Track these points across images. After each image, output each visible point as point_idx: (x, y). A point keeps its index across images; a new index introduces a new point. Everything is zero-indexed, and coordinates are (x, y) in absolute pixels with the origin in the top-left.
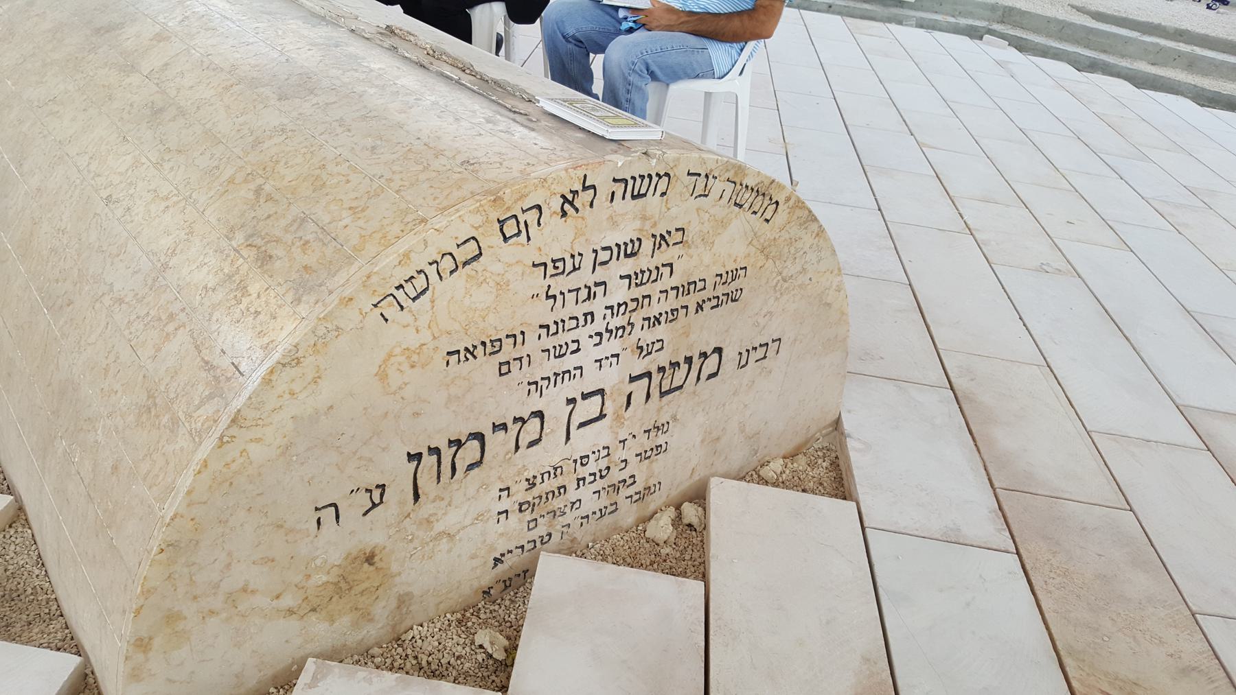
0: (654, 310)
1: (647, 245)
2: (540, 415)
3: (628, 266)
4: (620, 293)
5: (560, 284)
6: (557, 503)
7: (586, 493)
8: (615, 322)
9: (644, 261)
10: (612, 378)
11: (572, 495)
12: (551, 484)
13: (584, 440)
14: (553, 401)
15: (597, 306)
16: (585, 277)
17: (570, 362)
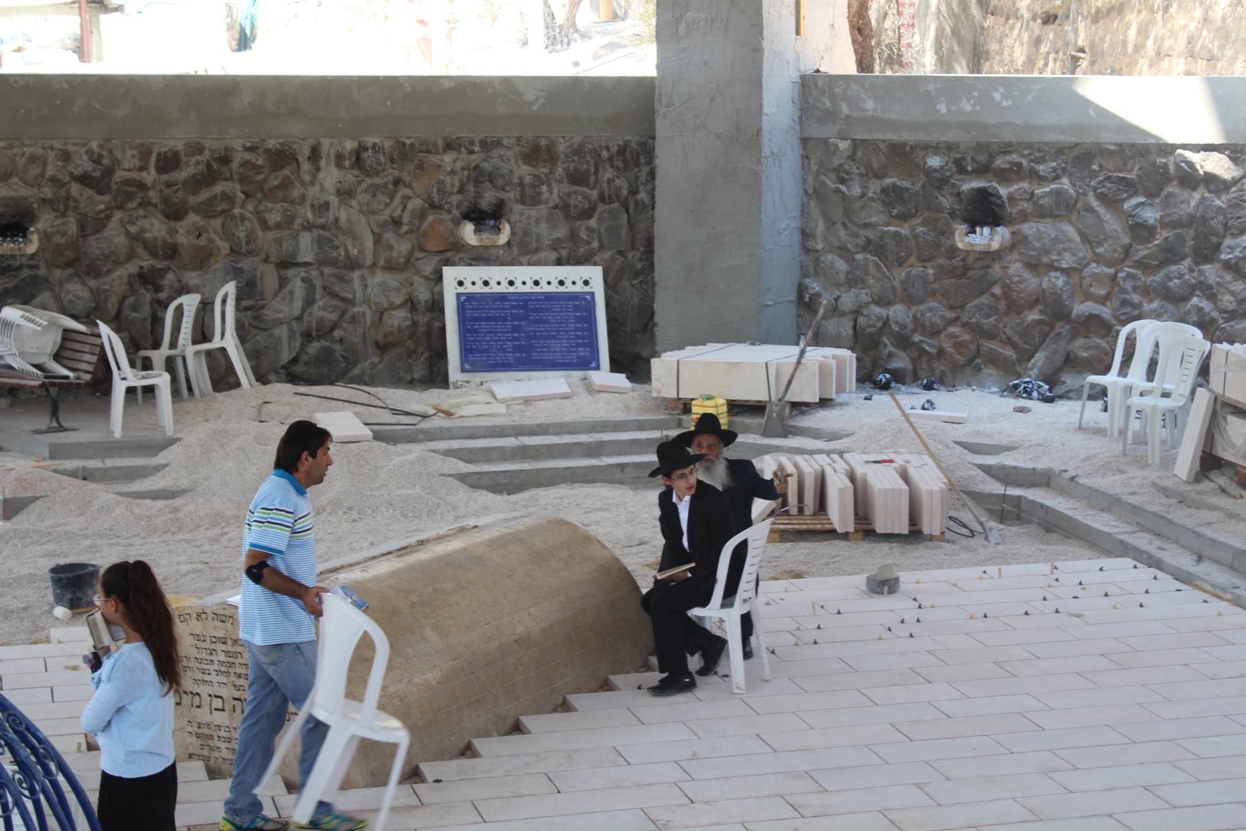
0: (239, 671)
1: (230, 642)
2: (198, 694)
3: (223, 647)
4: (222, 658)
5: (200, 644)
6: (210, 742)
7: (223, 746)
8: (223, 669)
9: (229, 647)
10: (224, 692)
11: (218, 744)
12: (205, 731)
13: (219, 718)
14: (204, 690)
15: (214, 658)
16: (207, 645)
17: (207, 678)
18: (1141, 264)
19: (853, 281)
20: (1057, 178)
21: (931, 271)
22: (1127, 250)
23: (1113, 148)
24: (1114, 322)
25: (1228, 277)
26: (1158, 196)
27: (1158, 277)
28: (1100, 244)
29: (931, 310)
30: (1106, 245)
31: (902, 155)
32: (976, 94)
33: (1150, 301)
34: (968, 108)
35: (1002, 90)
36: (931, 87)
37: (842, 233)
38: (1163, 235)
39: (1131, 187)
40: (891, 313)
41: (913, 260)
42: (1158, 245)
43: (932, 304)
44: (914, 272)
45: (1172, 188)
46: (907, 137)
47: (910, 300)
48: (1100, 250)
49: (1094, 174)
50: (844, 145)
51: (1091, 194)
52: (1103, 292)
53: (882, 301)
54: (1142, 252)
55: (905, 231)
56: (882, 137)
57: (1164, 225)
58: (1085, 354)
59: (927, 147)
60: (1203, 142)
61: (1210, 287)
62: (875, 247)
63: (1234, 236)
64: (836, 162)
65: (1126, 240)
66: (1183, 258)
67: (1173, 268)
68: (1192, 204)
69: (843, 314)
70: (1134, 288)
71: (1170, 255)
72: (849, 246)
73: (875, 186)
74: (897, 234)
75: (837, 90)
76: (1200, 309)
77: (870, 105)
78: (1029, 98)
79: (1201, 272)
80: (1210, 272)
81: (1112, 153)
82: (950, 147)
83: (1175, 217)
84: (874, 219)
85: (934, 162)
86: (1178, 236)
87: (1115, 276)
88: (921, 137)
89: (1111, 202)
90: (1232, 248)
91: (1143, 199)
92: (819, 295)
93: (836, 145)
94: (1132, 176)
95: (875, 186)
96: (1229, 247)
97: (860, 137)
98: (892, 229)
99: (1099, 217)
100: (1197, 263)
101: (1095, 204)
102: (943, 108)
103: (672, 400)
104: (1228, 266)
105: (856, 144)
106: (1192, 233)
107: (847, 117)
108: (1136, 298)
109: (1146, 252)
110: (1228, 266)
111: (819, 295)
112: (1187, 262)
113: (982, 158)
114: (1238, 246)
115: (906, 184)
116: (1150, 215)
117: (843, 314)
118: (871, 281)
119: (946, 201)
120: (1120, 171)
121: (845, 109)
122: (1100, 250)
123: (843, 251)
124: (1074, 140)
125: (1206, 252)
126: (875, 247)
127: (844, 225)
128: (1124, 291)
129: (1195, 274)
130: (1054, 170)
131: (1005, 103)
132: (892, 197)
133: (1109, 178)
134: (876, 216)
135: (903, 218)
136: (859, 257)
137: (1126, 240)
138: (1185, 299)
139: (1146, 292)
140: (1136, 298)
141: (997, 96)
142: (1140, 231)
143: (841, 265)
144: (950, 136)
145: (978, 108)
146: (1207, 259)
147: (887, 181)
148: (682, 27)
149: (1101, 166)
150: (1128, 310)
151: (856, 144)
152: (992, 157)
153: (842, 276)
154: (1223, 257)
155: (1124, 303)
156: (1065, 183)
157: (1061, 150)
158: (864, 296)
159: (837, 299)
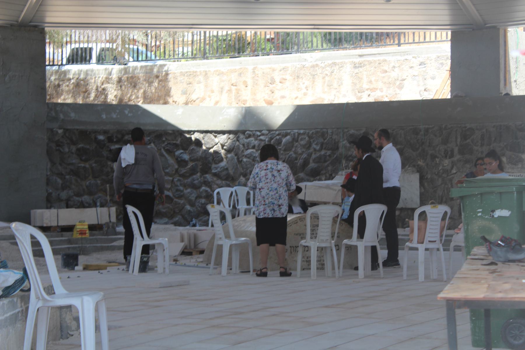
18: (183, 176)
19: (63, 188)
20: (150, 143)
21: (99, 182)
22: (177, 171)
23: (170, 132)
24: (173, 198)
25: (215, 179)
26: (187, 150)
27: (189, 180)
28: (167, 168)
29: (100, 197)
30: (169, 169)
31: (84, 135)
32: (118, 111)
33: (186, 189)
34: (115, 116)
35: (128, 110)
36: (99, 108)
37: (60, 167)
38: (191, 164)
39: (177, 146)
40: (83, 199)
41: (90, 177)
42: (189, 168)
43: (100, 195)
44: (92, 182)
45: (193, 147)
46: (89, 128)
47: (90, 194)
48: (167, 171)
49: (164, 142)
50: (60, 131)
51: (162, 149)
52: (169, 186)
53: (78, 195)
54: (183, 171)
55: (87, 166)
56: (78, 128)
57: (191, 160)
58: (164, 211)
59: (96, 132)
60: (205, 129)
61: (209, 183)
62: (75, 173)
63: (216, 163)
64: (57, 138)
65: (176, 167)
66: (197, 173)
67: (195, 176)
68: (201, 152)
69: (62, 200)
70: (181, 185)
71: (193, 171)
72: (63, 173)
73: (74, 148)
74: (84, 167)
75: (58, 109)
76: (206, 191)
77: (73, 115)
78: (139, 113)
79: (205, 178)
80: (208, 177)
81: (171, 134)
82: (105, 132)
83: (196, 157)
84: (74, 161)
85: (101, 137)
86: (196, 164)
87: (173, 181)
88: (95, 127)
89: (169, 152)
90: (216, 168)
91: (182, 151)
92: (51, 193)
93: (57, 132)
94: (178, 142)
95: (74, 148)
96: (215, 168)
97: (69, 128)
98: (83, 165)
99: (166, 158)
100: (203, 175)
101: (165, 153)
102: (104, 116)
103: (55, 227)
104: (215, 175)
105: (66, 130)
106: (200, 163)
107: (63, 120)
108: (181, 188)
109: (185, 171)
110: (215, 175)
111: (51, 193)
112: (199, 174)
113: (119, 136)
114: (218, 167)
115: (88, 147)
116: (186, 157)
117: (62, 200)
118: (73, 187)
119: (105, 153)
120: (173, 140)
121: (62, 116)
122: (167, 171)
123: (60, 175)
124: (157, 129)
125: (206, 170)
126: (75, 173)
127: (61, 164)
128: (177, 186)
129: (202, 178)
130: (149, 140)
131: (129, 115)
132: (81, 153)
133: (169, 143)
134: (75, 160)
135: (86, 161)
136: (67, 177)
137: (176, 167)
138: (199, 187)
139: (185, 186)
140: (181, 188)
141: (126, 112)
142: (181, 163)
143: (59, 181)
144: (107, 128)
145: (119, 116)
146: (206, 173)
147: (80, 146)
148: (7, 78)
149: (166, 139)
150: (179, 193)
151: (66, 130)
152: (123, 136)
153: (60, 185)
154: (213, 171)
155: (177, 190)
156: (152, 145)
157: (150, 133)
158: (71, 193)
159: (59, 195)
